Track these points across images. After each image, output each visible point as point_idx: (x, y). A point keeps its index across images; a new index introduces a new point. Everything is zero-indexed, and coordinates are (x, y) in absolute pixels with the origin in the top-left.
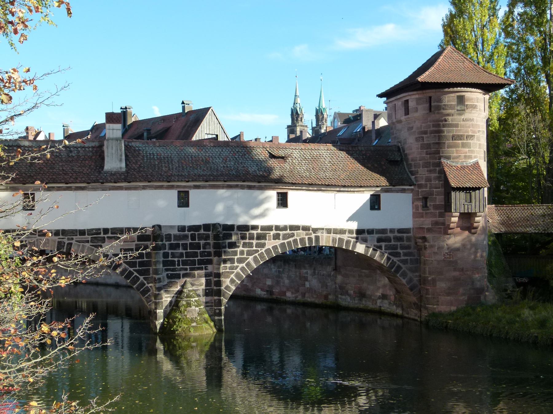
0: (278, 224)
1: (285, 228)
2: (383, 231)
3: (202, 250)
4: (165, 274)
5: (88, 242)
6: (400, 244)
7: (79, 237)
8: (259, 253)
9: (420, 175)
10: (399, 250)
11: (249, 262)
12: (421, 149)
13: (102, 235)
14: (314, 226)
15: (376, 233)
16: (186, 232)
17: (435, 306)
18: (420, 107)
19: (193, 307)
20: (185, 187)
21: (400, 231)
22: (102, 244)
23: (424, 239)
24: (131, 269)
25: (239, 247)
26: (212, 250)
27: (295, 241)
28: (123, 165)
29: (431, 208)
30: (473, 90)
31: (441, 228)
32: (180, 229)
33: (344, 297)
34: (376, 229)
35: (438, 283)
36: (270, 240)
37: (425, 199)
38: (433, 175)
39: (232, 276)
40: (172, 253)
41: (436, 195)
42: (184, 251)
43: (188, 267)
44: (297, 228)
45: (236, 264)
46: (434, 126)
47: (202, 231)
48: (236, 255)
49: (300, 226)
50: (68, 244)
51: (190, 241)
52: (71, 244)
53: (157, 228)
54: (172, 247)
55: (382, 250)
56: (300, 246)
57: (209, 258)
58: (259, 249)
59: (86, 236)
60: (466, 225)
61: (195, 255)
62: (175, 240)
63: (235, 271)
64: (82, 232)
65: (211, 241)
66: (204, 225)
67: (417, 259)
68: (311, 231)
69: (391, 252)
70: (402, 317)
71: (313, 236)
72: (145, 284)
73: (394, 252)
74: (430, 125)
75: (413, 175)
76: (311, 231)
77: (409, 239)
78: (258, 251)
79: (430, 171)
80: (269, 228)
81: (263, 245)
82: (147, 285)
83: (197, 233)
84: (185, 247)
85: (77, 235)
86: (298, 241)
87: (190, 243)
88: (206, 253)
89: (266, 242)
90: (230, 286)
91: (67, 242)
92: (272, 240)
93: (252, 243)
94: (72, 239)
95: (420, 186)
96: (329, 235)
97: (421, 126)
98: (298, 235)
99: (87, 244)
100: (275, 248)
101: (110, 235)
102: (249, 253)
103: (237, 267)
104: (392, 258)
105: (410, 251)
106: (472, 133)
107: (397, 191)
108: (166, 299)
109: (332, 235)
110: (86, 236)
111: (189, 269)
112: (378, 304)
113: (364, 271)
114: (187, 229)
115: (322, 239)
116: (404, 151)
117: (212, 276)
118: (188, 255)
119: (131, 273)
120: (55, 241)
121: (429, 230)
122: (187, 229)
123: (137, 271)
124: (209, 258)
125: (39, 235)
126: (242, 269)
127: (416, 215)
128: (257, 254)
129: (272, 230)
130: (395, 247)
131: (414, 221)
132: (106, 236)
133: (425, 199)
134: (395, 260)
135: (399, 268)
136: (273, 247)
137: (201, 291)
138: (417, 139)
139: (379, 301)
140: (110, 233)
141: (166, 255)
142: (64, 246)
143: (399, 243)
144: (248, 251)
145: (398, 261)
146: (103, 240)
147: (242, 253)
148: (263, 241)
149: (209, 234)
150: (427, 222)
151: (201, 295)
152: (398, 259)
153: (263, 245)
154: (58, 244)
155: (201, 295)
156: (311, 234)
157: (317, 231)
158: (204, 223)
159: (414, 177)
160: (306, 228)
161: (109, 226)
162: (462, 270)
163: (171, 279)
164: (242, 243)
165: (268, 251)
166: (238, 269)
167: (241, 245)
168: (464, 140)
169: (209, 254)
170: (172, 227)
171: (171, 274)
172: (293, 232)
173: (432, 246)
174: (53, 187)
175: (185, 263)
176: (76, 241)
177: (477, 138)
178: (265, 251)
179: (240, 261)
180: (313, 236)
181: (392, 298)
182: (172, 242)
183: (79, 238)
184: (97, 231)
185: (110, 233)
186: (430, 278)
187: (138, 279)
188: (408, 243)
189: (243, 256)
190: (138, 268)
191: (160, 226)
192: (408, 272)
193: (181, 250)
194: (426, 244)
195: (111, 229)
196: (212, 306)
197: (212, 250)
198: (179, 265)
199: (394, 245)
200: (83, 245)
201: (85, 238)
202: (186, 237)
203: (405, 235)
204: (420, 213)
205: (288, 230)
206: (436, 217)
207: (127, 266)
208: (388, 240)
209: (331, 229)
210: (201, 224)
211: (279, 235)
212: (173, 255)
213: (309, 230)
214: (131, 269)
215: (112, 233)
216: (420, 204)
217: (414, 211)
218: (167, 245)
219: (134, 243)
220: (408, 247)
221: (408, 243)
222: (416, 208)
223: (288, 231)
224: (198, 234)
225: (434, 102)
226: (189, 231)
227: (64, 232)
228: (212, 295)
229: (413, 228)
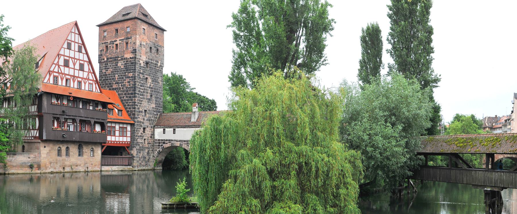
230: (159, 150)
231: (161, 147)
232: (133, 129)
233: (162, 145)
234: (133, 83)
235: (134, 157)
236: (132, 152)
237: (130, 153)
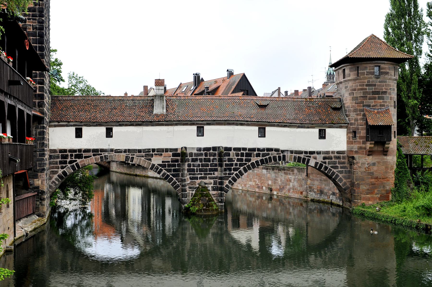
0: (259, 147)
1: (263, 150)
2: (327, 152)
3: (211, 163)
4: (188, 177)
5: (143, 156)
6: (338, 161)
7: (138, 154)
8: (247, 165)
9: (351, 117)
10: (337, 165)
11: (240, 171)
12: (352, 101)
13: (151, 153)
14: (282, 148)
15: (323, 154)
16: (202, 152)
17: (359, 201)
18: (351, 73)
20: (201, 124)
21: (338, 152)
22: (151, 158)
23: (353, 158)
24: (169, 173)
25: (234, 161)
26: (217, 163)
28: (165, 111)
29: (358, 138)
30: (386, 62)
31: (363, 151)
32: (198, 150)
33: (311, 193)
34: (322, 151)
35: (361, 186)
36: (254, 157)
37: (355, 132)
38: (359, 117)
39: (230, 179)
40: (193, 164)
41: (361, 130)
42: (200, 163)
43: (203, 173)
44: (271, 150)
45: (232, 172)
46: (360, 85)
47: (211, 151)
48: (233, 166)
49: (273, 149)
50: (131, 158)
51: (204, 157)
52: (133, 158)
53: (184, 149)
54: (193, 160)
55: (326, 164)
57: (216, 167)
58: (247, 163)
59: (142, 153)
60: (380, 149)
61: (207, 165)
62: (195, 156)
63: (232, 176)
64: (140, 151)
65: (217, 157)
66: (212, 147)
67: (350, 170)
68: (280, 152)
69: (332, 166)
70: (342, 207)
71: (281, 155)
72: (177, 183)
73: (334, 166)
74: (358, 85)
75: (347, 117)
76: (280, 152)
77: (344, 158)
78: (246, 164)
79: (357, 115)
80: (254, 150)
82: (178, 183)
83: (208, 152)
84: (201, 160)
85: (137, 153)
86: (272, 158)
87: (204, 158)
88: (214, 165)
89: (252, 158)
90: (229, 185)
91: (131, 157)
92: (255, 157)
94: (134, 155)
95: (351, 124)
96: (292, 154)
97: (352, 86)
98: (272, 155)
99: (143, 158)
101: (156, 153)
102: (241, 165)
103: (233, 173)
104: (333, 169)
105: (345, 165)
106: (385, 90)
107: (337, 127)
108: (189, 192)
109: (294, 155)
110: (142, 153)
111: (203, 174)
112: (331, 198)
113: (323, 177)
114: (202, 149)
115: (287, 157)
116: (343, 102)
117: (217, 179)
118: (203, 165)
119: (168, 176)
120: (124, 156)
121: (356, 152)
122: (202, 149)
123: (172, 175)
124: (216, 167)
125: (115, 152)
127: (349, 143)
128: (245, 166)
129: (255, 151)
130: (335, 163)
131: (347, 146)
132: (153, 153)
133: (355, 132)
134: (334, 171)
135: (337, 176)
137: (211, 187)
138: (350, 94)
139: (331, 196)
140: (156, 151)
141: (189, 165)
142: (129, 159)
143: (337, 160)
144: (240, 164)
145: (337, 171)
146: (152, 156)
147: (236, 165)
149: (216, 153)
150: (355, 147)
151: (211, 190)
152: (337, 170)
153: (250, 160)
154: (126, 158)
155: (211, 190)
157: (284, 152)
158: (213, 146)
159: (348, 118)
160: (277, 150)
161: (156, 147)
162: (377, 178)
163: (193, 180)
164: (236, 159)
166: (234, 175)
167: (236, 160)
168: (379, 94)
169: (216, 165)
170: (193, 148)
171: (192, 177)
172: (268, 152)
173: (357, 163)
174: (123, 124)
175: (201, 170)
176: (136, 156)
177: (389, 93)
179: (235, 170)
180: (281, 155)
181: (338, 195)
182: (193, 157)
183: (138, 154)
184: (149, 150)
185: (156, 151)
186: (356, 183)
187: (173, 179)
188: (343, 160)
189: (237, 167)
190: (172, 173)
191: (186, 148)
192: (343, 179)
193: (198, 163)
194: (354, 161)
195: (157, 149)
196: (217, 197)
197: (217, 163)
198: (197, 171)
199: (334, 161)
200: (140, 158)
201: (141, 154)
202: (201, 154)
203: (341, 155)
204: (351, 141)
205: (266, 151)
206: (360, 144)
207: (166, 172)
208: (331, 158)
209: (293, 151)
210: (211, 147)
212: (194, 166)
214: (169, 173)
215: (157, 152)
216: (351, 135)
217: (348, 140)
218: (190, 159)
219: (170, 158)
220: (344, 163)
221: (343, 160)
222: (348, 138)
224: (209, 153)
225: (360, 70)
226: (203, 151)
227: (129, 151)
228: (217, 190)
229: (347, 151)
230: (64, 173)
231: (69, 165)
232: (39, 130)
233: (71, 162)
234: (36, 24)
235: (43, 192)
236: (37, 182)
237: (31, 185)
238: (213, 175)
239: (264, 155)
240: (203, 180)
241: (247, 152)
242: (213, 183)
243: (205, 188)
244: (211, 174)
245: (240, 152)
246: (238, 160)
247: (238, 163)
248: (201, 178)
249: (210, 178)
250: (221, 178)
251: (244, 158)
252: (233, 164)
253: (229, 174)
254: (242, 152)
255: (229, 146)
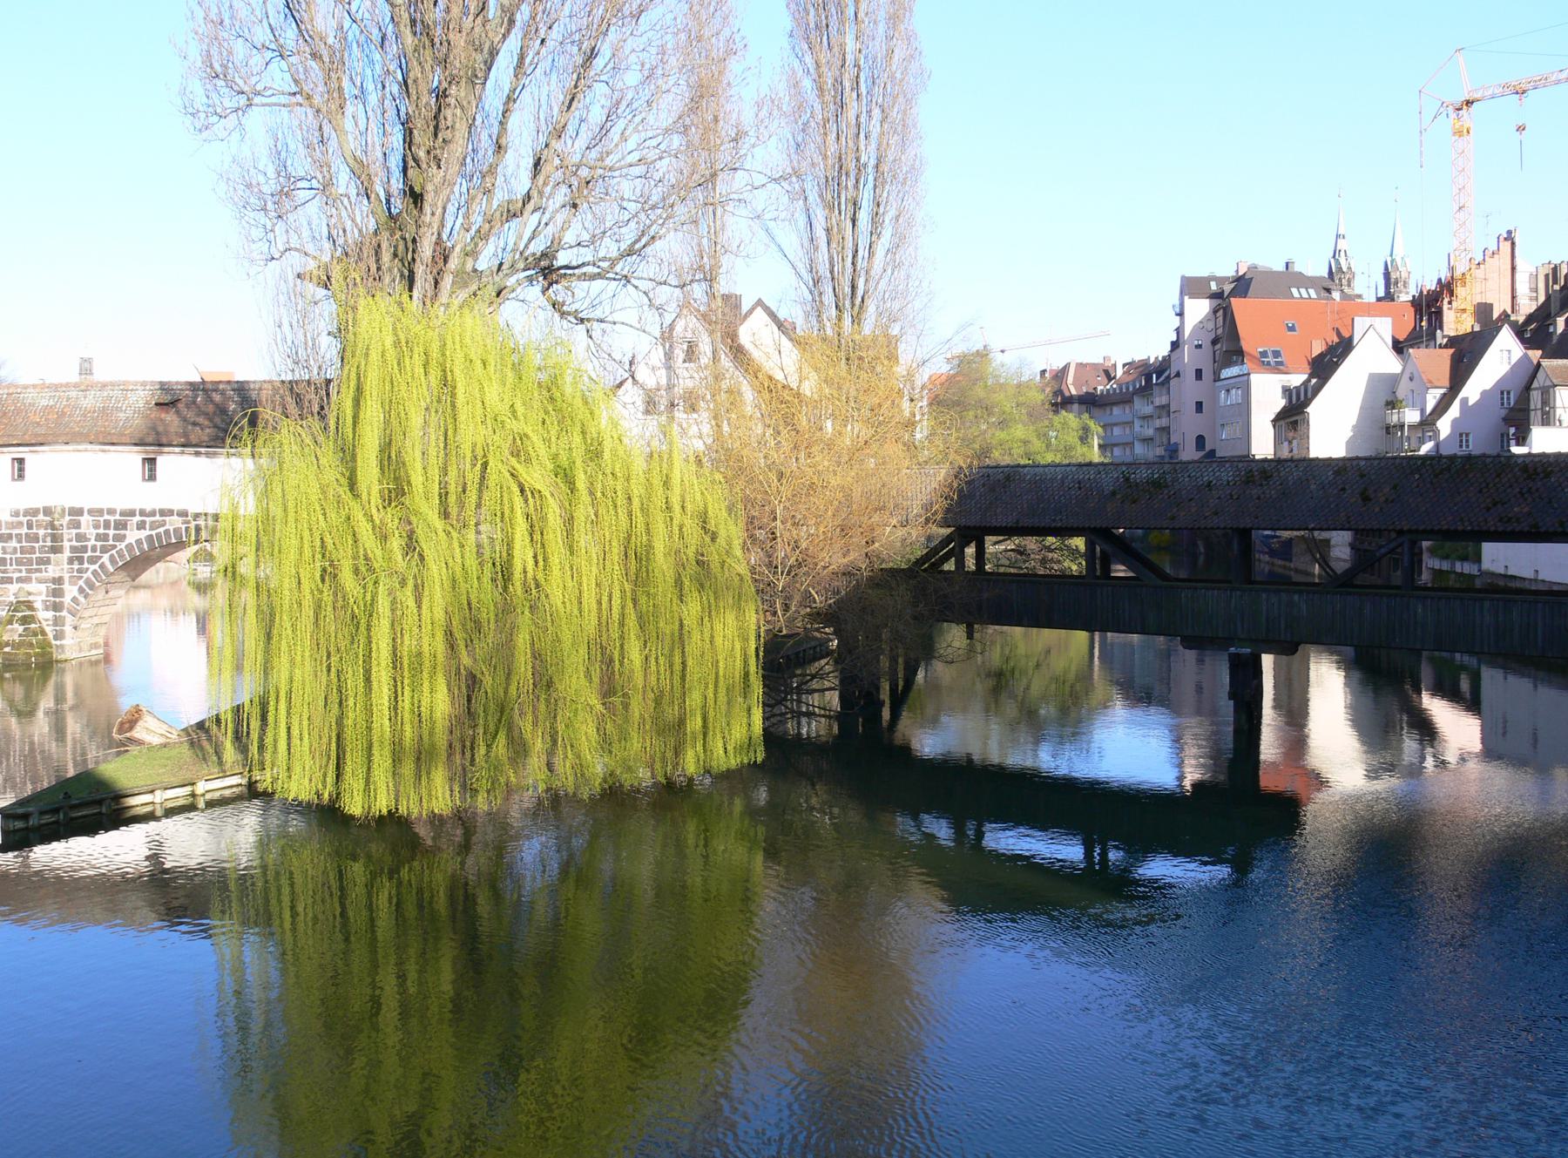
0: (143, 507)
1: (153, 513)
19: (16, 626)
27: (167, 532)
36: (132, 530)
39: (81, 583)
45: (86, 565)
48: (86, 552)
56: (174, 541)
58: (117, 544)
63: (85, 576)
71: (193, 525)
76: (189, 518)
80: (132, 513)
81: (120, 538)
89: (127, 533)
93: (108, 535)
98: (171, 525)
100: (139, 542)
102: (104, 550)
103: (87, 569)
126: (95, 573)
128: (114, 552)
129: (135, 515)
136: (137, 541)
144: (102, 546)
147: (94, 549)
148: (122, 532)
156: (188, 522)
160: (183, 514)
165: (129, 547)
167: (93, 538)
175: (19, 562)
178: (126, 546)
198: (11, 565)
211: (144, 522)
213: (187, 516)
223: (158, 518)
238: (44, 574)
239: (153, 526)
240: (24, 585)
241: (118, 517)
242: (45, 593)
243: (29, 605)
244: (39, 571)
245: (102, 519)
246: (99, 537)
247: (99, 544)
248: (20, 580)
249: (40, 581)
250: (59, 581)
251: (111, 532)
252: (86, 547)
253: (79, 571)
254: (107, 517)
255: (77, 505)
